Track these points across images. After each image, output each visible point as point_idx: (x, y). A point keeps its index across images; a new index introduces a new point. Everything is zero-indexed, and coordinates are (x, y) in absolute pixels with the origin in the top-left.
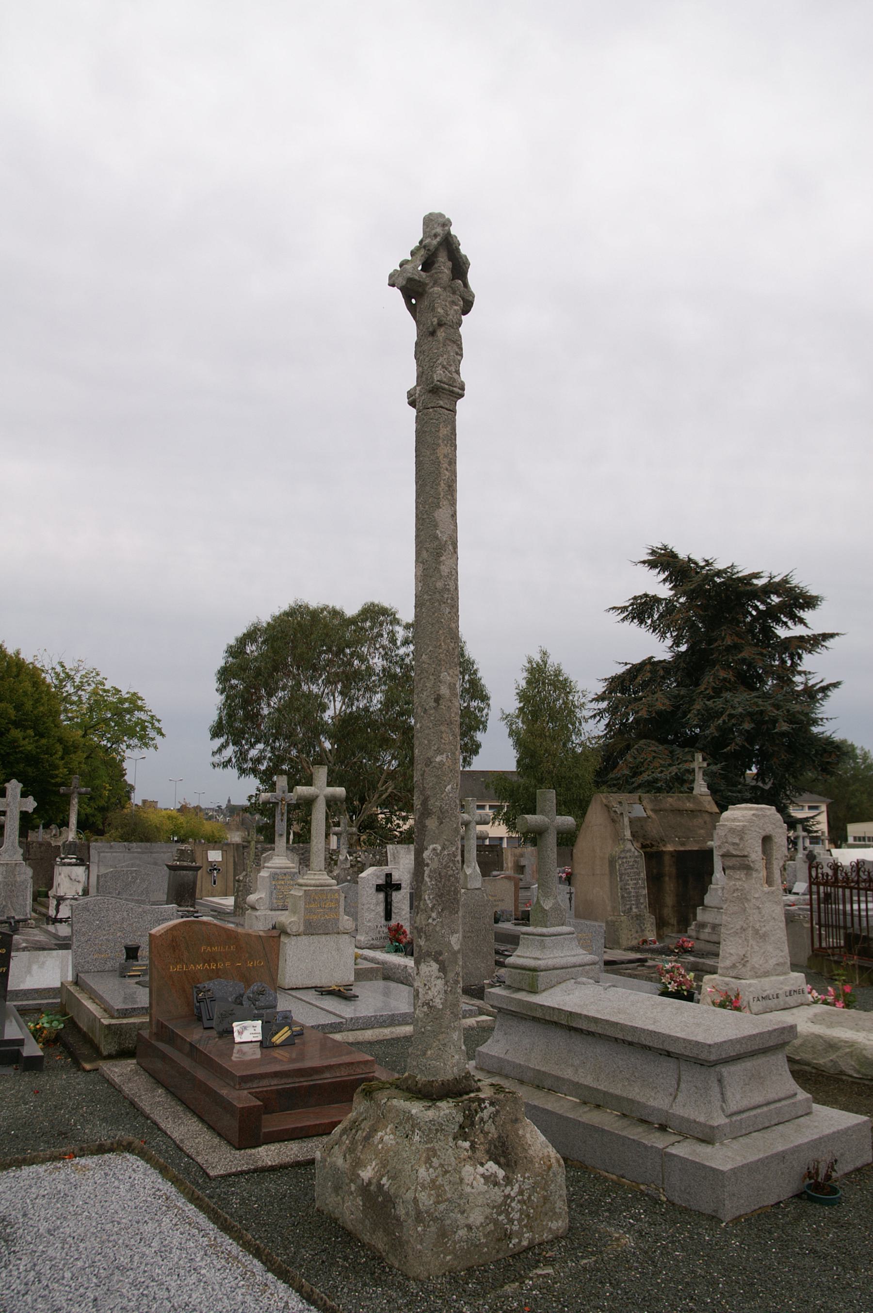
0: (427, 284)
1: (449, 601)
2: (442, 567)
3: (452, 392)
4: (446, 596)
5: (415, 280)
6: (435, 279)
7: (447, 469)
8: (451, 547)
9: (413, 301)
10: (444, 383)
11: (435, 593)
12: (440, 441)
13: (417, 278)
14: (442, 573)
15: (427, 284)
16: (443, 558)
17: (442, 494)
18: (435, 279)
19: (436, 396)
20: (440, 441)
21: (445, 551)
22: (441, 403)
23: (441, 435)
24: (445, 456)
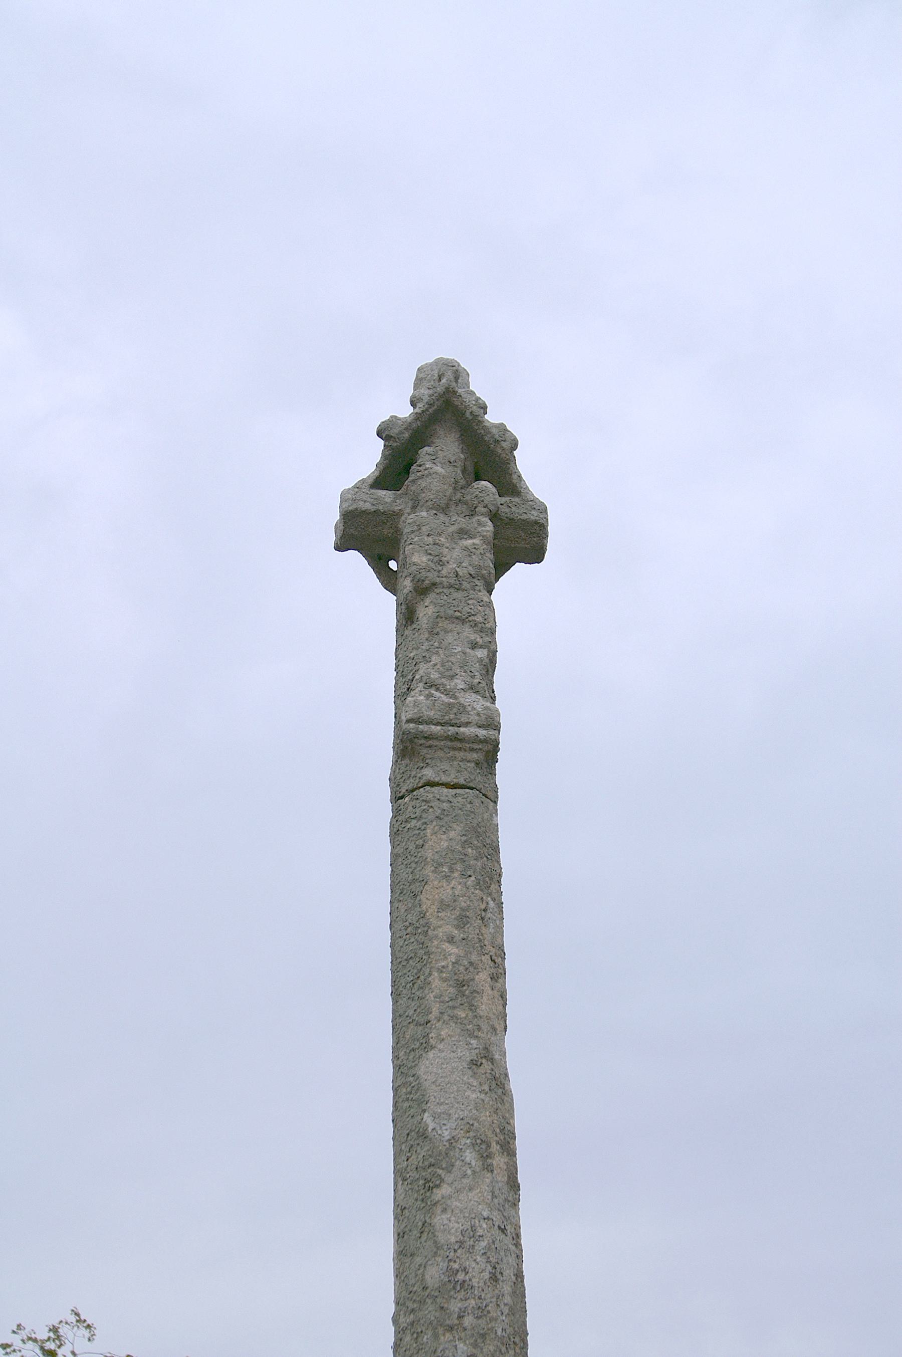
0: (398, 514)
1: (468, 1321)
2: (439, 1219)
3: (456, 738)
4: (455, 1306)
5: (364, 512)
6: (445, 499)
7: (451, 940)
8: (470, 1156)
9: (393, 565)
10: (430, 722)
11: (422, 1302)
12: (428, 870)
13: (367, 506)
14: (441, 1238)
15: (398, 514)
16: (438, 1194)
17: (435, 1011)
18: (445, 499)
19: (445, 757)
20: (428, 870)
21: (449, 1169)
22: (429, 774)
23: (429, 854)
24: (443, 906)
